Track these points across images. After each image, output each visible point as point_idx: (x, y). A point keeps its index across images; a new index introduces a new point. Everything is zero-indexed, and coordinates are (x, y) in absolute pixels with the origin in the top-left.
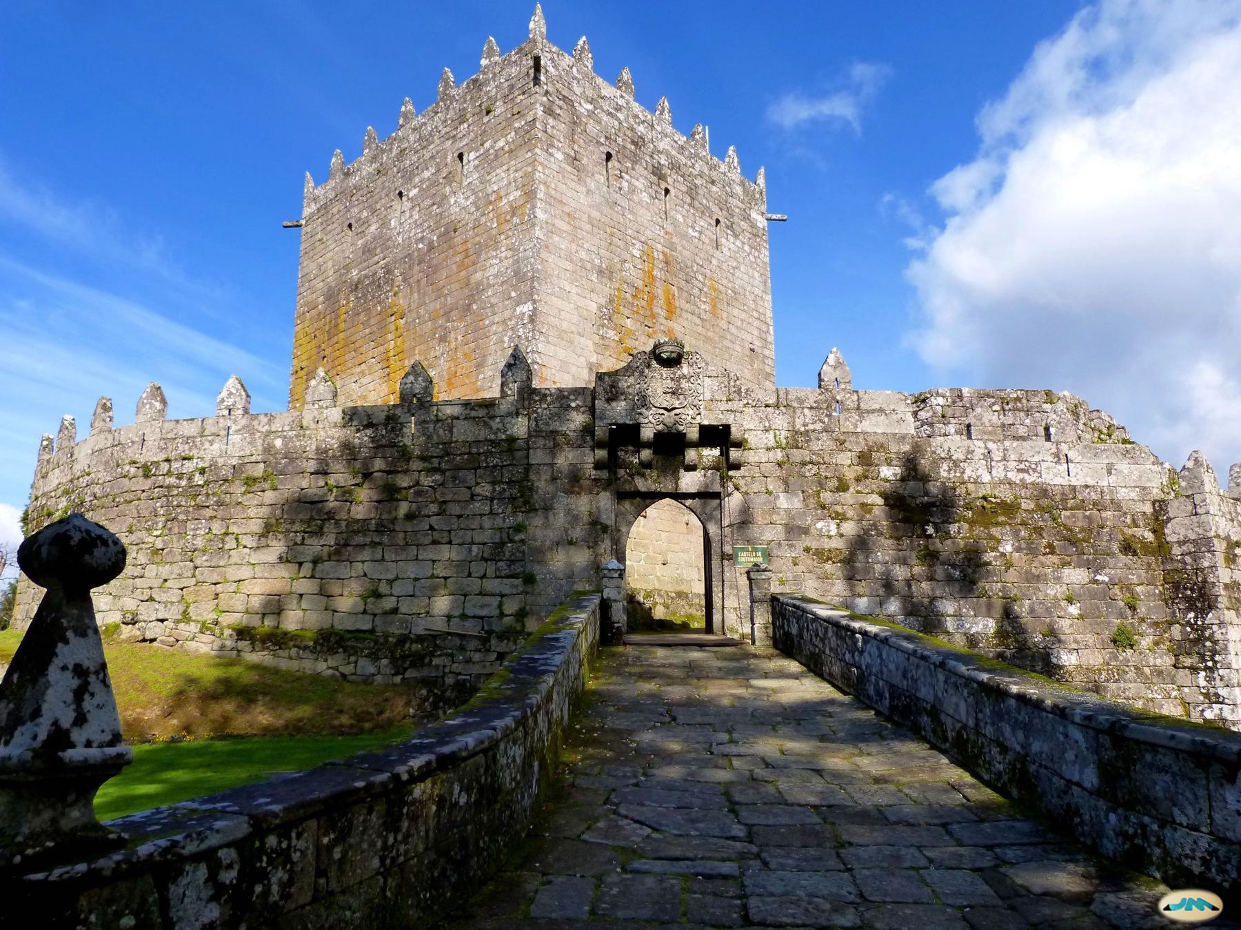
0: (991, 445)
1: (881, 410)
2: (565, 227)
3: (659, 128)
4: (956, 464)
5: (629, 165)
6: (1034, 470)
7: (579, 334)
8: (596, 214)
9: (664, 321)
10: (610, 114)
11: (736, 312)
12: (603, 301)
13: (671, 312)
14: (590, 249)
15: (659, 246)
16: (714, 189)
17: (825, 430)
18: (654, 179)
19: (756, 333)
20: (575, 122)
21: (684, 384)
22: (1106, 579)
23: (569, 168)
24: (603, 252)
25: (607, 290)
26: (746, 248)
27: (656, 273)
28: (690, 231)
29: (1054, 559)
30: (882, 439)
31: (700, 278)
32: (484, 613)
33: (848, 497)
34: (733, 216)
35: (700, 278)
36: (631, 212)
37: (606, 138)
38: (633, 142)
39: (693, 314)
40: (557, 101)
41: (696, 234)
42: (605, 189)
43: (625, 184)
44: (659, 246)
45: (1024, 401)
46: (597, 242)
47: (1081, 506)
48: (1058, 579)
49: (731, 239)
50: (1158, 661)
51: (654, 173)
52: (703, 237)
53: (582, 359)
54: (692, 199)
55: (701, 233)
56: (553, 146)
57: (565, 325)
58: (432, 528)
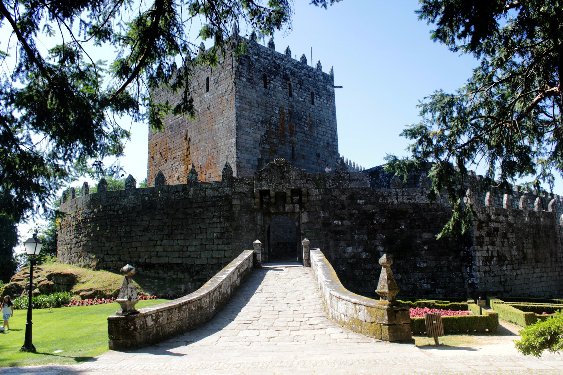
0: (397, 190)
1: (358, 180)
2: (247, 107)
3: (286, 59)
4: (385, 198)
5: (273, 77)
6: (413, 198)
8: (259, 100)
9: (289, 137)
10: (265, 58)
11: (320, 129)
12: (263, 133)
13: (292, 133)
15: (287, 108)
16: (311, 79)
17: (337, 188)
18: (284, 80)
19: (330, 136)
21: (285, 174)
23: (248, 84)
24: (263, 114)
25: (265, 128)
26: (325, 101)
27: (285, 118)
28: (300, 99)
29: (420, 230)
30: (358, 190)
31: (305, 117)
32: (219, 256)
33: (345, 211)
34: (319, 89)
35: (305, 117)
36: (274, 96)
37: (264, 68)
38: (275, 67)
39: (301, 132)
40: (243, 58)
41: (303, 100)
42: (263, 89)
43: (272, 85)
44: (287, 108)
46: (260, 110)
47: (430, 210)
48: (421, 237)
49: (318, 99)
51: (284, 78)
52: (306, 100)
53: (255, 158)
54: (301, 85)
55: (304, 99)
56: (241, 76)
57: (248, 146)
58: (200, 228)
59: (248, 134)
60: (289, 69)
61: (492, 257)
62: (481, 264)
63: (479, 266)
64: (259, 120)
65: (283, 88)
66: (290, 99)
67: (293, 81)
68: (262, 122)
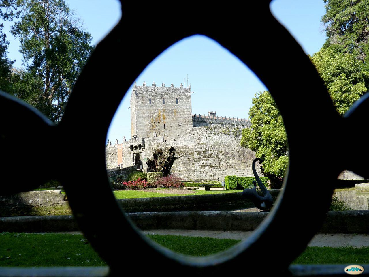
2: (142, 113)
5: (155, 98)
7: (145, 128)
8: (147, 109)
13: (164, 118)
14: (147, 114)
21: (137, 140)
25: (150, 119)
28: (170, 103)
35: (172, 110)
38: (156, 94)
57: (142, 127)
59: (142, 123)
60: (163, 92)
61: (206, 166)
62: (198, 168)
63: (197, 169)
65: (160, 101)
66: (164, 105)
67: (166, 97)
68: (148, 117)
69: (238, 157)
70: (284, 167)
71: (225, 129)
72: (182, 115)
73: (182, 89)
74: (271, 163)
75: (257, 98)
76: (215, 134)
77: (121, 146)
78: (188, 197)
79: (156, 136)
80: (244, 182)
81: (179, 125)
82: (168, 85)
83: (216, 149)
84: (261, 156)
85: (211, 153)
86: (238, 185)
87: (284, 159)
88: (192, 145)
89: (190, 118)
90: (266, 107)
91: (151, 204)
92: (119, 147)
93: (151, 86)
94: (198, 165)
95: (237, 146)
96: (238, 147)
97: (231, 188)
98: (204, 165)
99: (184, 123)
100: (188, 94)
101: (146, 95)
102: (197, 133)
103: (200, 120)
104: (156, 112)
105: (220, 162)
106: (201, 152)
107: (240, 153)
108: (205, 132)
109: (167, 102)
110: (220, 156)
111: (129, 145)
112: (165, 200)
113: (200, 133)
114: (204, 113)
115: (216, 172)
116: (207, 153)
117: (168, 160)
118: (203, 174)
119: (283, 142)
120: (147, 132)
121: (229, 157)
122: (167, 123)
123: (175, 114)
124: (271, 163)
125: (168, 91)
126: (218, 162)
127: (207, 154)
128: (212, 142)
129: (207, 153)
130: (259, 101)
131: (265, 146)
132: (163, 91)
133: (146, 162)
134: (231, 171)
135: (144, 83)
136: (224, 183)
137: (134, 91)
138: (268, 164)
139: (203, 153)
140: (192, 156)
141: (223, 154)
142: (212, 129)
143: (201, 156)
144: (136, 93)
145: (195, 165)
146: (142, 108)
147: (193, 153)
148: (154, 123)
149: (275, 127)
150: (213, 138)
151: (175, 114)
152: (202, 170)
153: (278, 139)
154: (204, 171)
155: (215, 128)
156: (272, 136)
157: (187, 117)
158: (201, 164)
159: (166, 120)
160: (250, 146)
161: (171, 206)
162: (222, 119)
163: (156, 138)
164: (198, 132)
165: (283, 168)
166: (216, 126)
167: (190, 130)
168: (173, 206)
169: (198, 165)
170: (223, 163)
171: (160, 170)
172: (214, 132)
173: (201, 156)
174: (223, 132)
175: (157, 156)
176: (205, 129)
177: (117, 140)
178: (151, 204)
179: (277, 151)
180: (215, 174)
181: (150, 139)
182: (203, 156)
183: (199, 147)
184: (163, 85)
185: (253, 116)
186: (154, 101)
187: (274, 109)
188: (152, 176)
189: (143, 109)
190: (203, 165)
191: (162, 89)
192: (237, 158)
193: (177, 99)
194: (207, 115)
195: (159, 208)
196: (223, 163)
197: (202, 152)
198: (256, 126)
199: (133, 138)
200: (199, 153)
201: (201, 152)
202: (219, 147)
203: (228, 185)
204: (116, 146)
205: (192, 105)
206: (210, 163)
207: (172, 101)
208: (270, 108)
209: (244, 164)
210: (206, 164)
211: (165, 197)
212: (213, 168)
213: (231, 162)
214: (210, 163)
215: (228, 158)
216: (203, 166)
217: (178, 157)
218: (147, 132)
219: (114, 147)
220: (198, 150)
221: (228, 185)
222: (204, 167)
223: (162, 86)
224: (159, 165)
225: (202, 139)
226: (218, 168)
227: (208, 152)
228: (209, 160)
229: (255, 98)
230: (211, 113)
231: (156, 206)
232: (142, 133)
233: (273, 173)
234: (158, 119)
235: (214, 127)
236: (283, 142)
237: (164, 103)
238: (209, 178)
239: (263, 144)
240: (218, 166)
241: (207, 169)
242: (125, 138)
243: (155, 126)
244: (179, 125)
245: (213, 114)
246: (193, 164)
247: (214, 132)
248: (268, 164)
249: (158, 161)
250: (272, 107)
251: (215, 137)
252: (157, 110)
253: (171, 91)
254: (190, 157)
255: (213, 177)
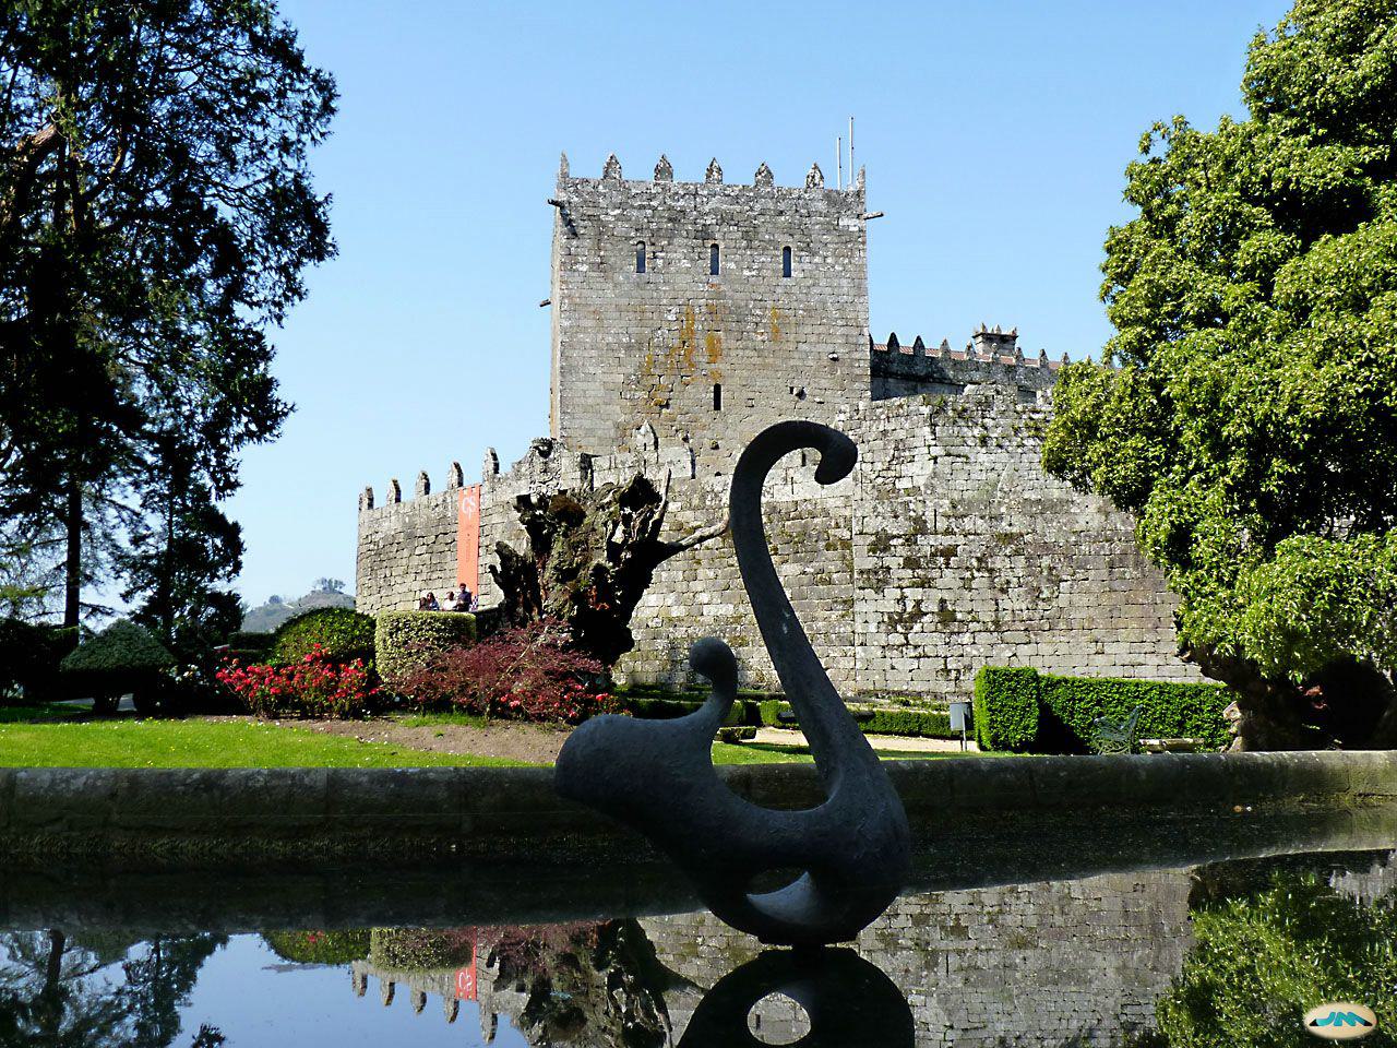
7: (607, 404)
8: (624, 301)
10: (644, 207)
11: (808, 329)
13: (714, 354)
14: (619, 330)
16: (783, 218)
20: (601, 232)
21: (551, 465)
22: (812, 570)
28: (746, 273)
35: (758, 312)
38: (670, 220)
45: (905, 407)
50: (842, 630)
53: (609, 423)
57: (590, 401)
60: (714, 211)
61: (918, 614)
62: (872, 628)
64: (620, 343)
65: (692, 260)
66: (714, 279)
67: (726, 237)
68: (629, 347)
69: (1105, 572)
70: (1305, 611)
71: (1041, 416)
72: (813, 338)
73: (816, 194)
74: (1230, 585)
75: (1155, 161)
76: (984, 441)
77: (475, 498)
78: (401, 778)
79: (656, 443)
80: (1087, 711)
81: (795, 392)
82: (740, 175)
83: (980, 522)
84: (1162, 538)
85: (948, 541)
86: (1048, 718)
87: (1308, 556)
88: (847, 497)
89: (857, 355)
90: (1207, 210)
91: (115, 817)
92: (467, 505)
93: (650, 177)
94: (874, 607)
95: (1099, 510)
96: (1107, 514)
97: (999, 744)
98: (909, 610)
99: (824, 383)
100: (849, 223)
101: (622, 228)
102: (885, 433)
103: (920, 370)
104: (671, 317)
105: (1000, 596)
106: (894, 537)
107: (1118, 548)
108: (927, 429)
109: (733, 266)
110: (998, 563)
111: (511, 496)
112: (217, 793)
113: (901, 434)
114: (944, 329)
115: (975, 652)
116: (926, 544)
117: (609, 558)
118: (898, 663)
119: (1302, 439)
120: (617, 426)
121: (1051, 569)
122: (730, 381)
123: (776, 334)
124: (1230, 585)
125: (738, 208)
126: (989, 594)
127: (927, 550)
128: (963, 485)
129: (926, 544)
130: (1166, 175)
131: (1193, 472)
132: (714, 203)
133: (493, 569)
134: (1063, 649)
135: (612, 163)
136: (963, 710)
137: (554, 203)
138: (1207, 589)
139: (901, 541)
140: (844, 557)
141: (1017, 553)
142: (965, 410)
143: (889, 561)
144: (564, 216)
145: (858, 607)
146: (594, 298)
147: (846, 544)
148: (655, 381)
149: (1258, 333)
150: (973, 460)
151: (776, 334)
152: (897, 639)
153: (1267, 417)
154: (908, 644)
155: (986, 404)
156: (1228, 398)
157: (841, 351)
158: (888, 602)
159: (721, 366)
160: (1098, 475)
161: (262, 843)
162: (1044, 365)
163: (650, 456)
164: (890, 427)
165: (1298, 619)
166: (991, 393)
167: (842, 417)
168: (278, 845)
169: (874, 607)
170: (1015, 602)
171: (560, 618)
172: (977, 431)
173: (893, 562)
174: (1028, 427)
175: (550, 534)
176: (926, 410)
177: (457, 466)
178: (115, 817)
179: (1266, 502)
180: (966, 660)
181: (623, 463)
182: (901, 561)
183: (880, 509)
184: (710, 171)
185: (1124, 278)
186: (660, 262)
187: (1262, 228)
188: (401, 636)
189: (598, 301)
190: (899, 609)
191: (706, 192)
192: (1097, 573)
193: (787, 250)
194: (960, 341)
195: (172, 851)
196: (1015, 602)
197: (899, 537)
198: (1140, 338)
199: (533, 454)
200: (881, 544)
201: (894, 537)
202: (994, 512)
203: (982, 719)
204: (449, 500)
205: (872, 284)
206: (943, 601)
207: (763, 259)
208: (1235, 215)
209: (1136, 611)
210: (918, 603)
211: (222, 774)
212: (955, 627)
213: (1063, 601)
214: (943, 601)
215: (1045, 573)
216: (900, 614)
217: (683, 543)
218: (617, 426)
219: (441, 499)
220: (873, 524)
221: (986, 721)
222: (903, 620)
223: (708, 177)
224: (559, 586)
225: (907, 469)
226: (987, 630)
227: (932, 540)
228: (939, 583)
229: (1145, 159)
230: (989, 338)
231: (155, 831)
232: (590, 432)
233: (1239, 648)
234: (681, 359)
235: (980, 404)
236: (1302, 439)
237: (715, 271)
238: (932, 686)
239: (1182, 463)
240: (987, 617)
241: (925, 634)
242: (495, 456)
243: (661, 397)
244: (795, 392)
245: (1004, 341)
246: (845, 602)
247: (977, 431)
248: (1207, 589)
249: (552, 563)
250: (1246, 208)
251: (982, 458)
252: (675, 309)
253: (758, 207)
254: (830, 562)
255: (957, 679)
